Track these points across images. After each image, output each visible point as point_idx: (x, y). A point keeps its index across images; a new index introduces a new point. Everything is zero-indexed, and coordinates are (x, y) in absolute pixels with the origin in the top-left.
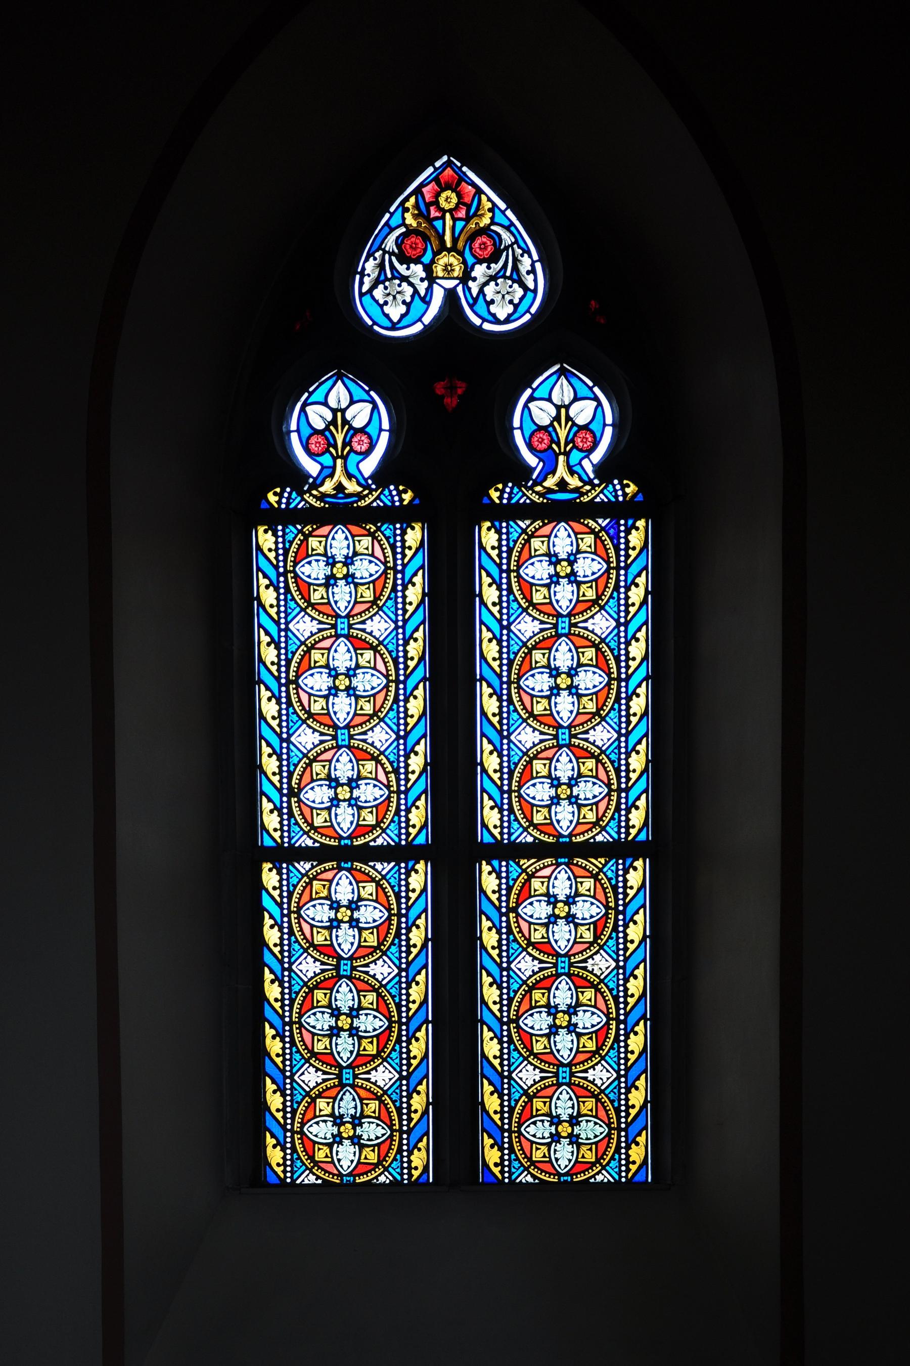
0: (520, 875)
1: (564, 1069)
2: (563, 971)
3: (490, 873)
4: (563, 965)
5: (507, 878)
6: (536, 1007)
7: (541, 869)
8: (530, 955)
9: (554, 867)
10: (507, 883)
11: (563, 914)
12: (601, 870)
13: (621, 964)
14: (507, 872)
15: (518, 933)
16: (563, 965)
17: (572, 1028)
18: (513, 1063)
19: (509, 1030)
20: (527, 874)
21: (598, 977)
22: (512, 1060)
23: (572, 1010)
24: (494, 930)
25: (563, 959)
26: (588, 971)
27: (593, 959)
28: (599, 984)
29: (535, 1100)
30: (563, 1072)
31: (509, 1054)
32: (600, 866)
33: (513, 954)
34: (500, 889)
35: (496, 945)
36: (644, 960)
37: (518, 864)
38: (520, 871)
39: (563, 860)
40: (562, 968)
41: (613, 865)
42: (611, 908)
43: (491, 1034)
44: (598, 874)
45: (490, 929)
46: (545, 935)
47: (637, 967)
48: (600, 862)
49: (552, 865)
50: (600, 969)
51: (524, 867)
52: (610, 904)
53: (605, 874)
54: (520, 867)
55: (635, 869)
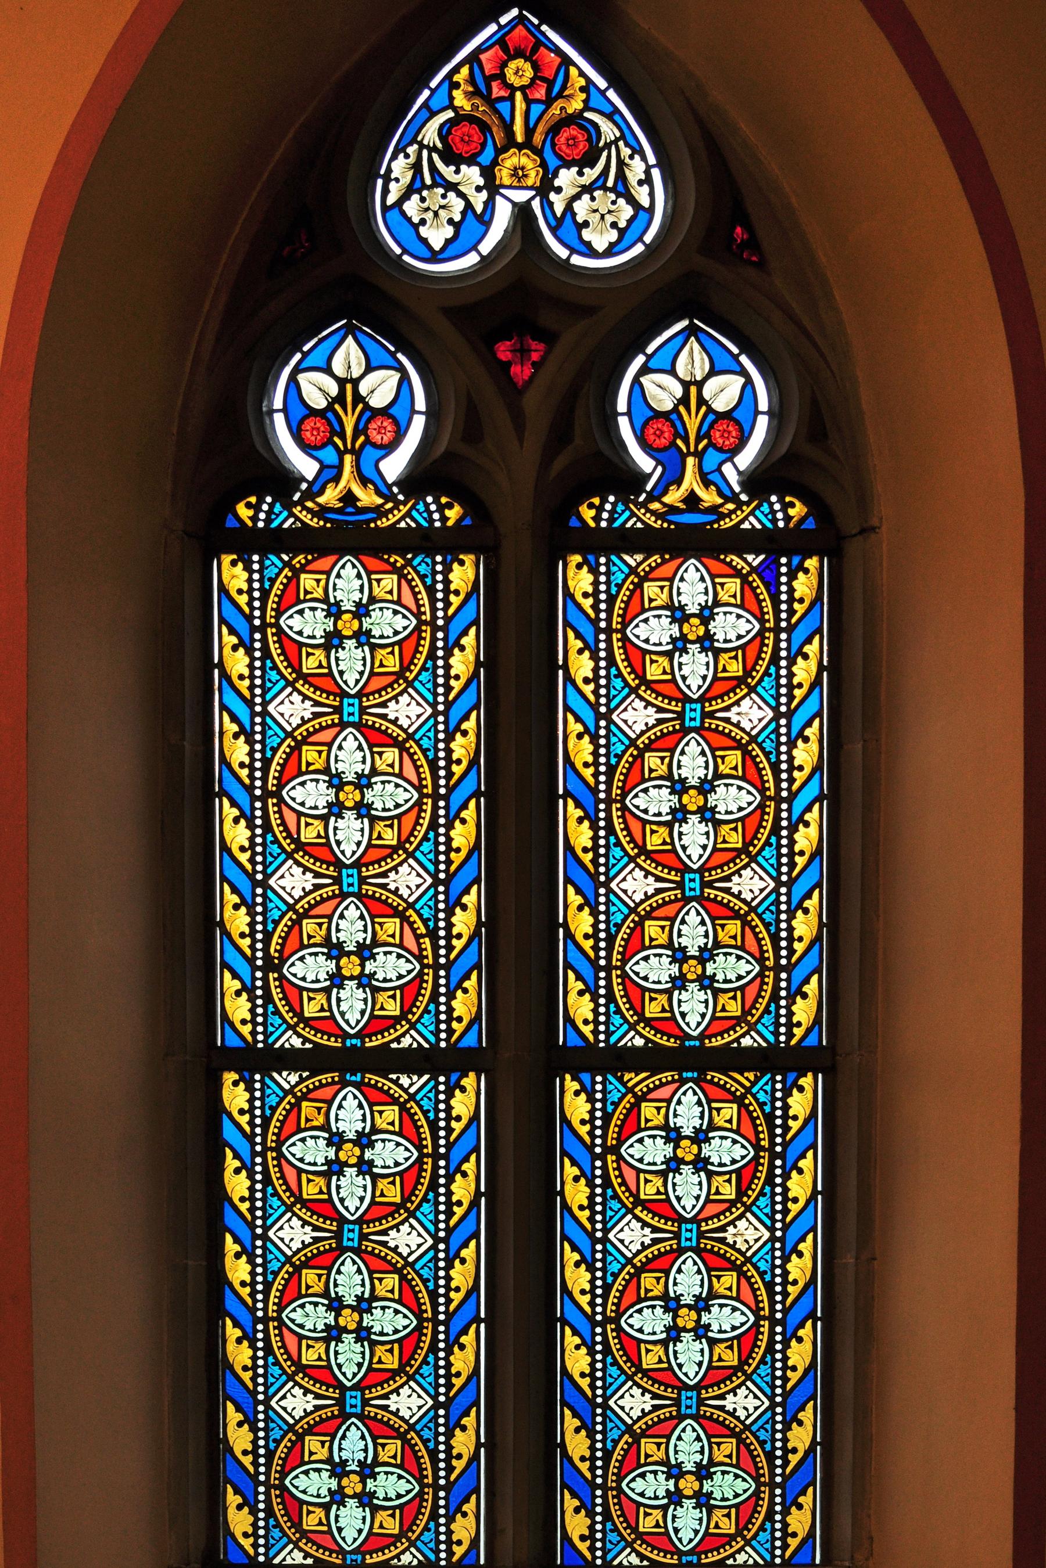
0: (624, 1096)
1: (689, 1394)
2: (688, 1244)
3: (577, 1093)
4: (689, 1235)
5: (604, 1101)
6: (647, 1299)
7: (656, 1088)
8: (638, 1219)
9: (676, 1085)
10: (603, 1109)
11: (689, 1158)
12: (748, 1090)
13: (779, 1234)
14: (604, 1091)
15: (620, 1185)
16: (689, 1235)
17: (701, 1331)
18: (611, 1384)
19: (604, 1334)
20: (635, 1095)
21: (743, 1254)
22: (609, 1380)
23: (701, 1304)
24: (583, 1181)
25: (689, 1226)
26: (728, 1245)
27: (735, 1227)
28: (743, 1264)
29: (643, 1441)
30: (687, 1398)
31: (604, 1370)
32: (748, 1084)
33: (611, 1218)
34: (593, 1118)
35: (585, 1203)
36: (814, 1229)
37: (620, 1080)
38: (623, 1090)
39: (690, 1075)
40: (687, 1239)
41: (766, 1084)
42: (763, 1148)
43: (577, 1340)
44: (744, 1096)
45: (576, 1179)
46: (662, 1190)
47: (803, 1239)
48: (747, 1079)
49: (673, 1081)
50: (746, 1241)
51: (630, 1084)
52: (763, 1143)
53: (754, 1096)
54: (624, 1084)
55: (801, 1089)
